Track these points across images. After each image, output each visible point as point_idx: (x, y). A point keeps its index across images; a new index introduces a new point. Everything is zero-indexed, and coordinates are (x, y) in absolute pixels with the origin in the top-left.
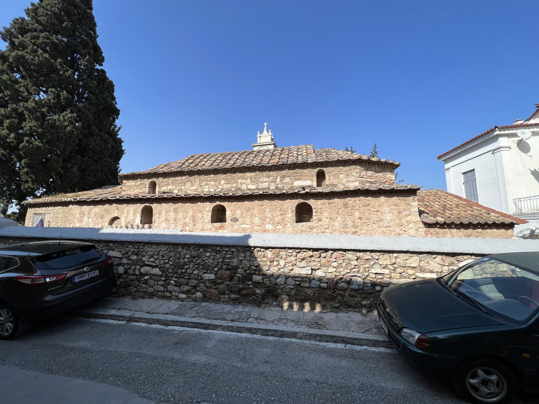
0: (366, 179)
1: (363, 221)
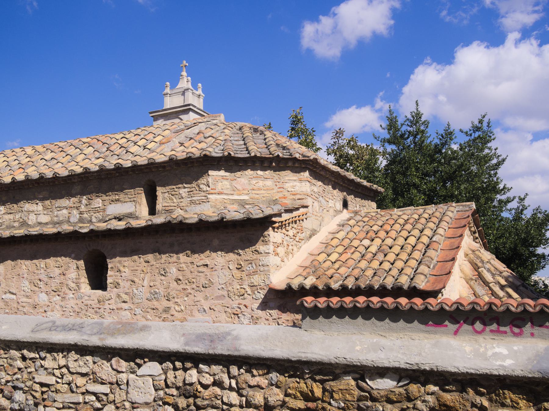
0: (231, 197)
1: (182, 286)
